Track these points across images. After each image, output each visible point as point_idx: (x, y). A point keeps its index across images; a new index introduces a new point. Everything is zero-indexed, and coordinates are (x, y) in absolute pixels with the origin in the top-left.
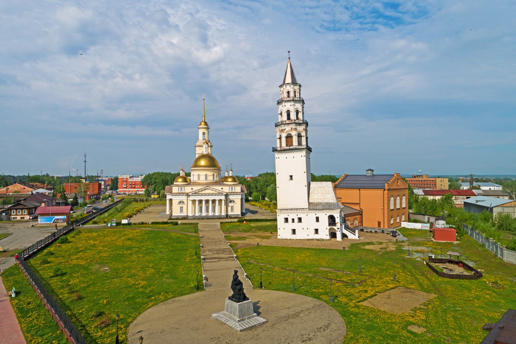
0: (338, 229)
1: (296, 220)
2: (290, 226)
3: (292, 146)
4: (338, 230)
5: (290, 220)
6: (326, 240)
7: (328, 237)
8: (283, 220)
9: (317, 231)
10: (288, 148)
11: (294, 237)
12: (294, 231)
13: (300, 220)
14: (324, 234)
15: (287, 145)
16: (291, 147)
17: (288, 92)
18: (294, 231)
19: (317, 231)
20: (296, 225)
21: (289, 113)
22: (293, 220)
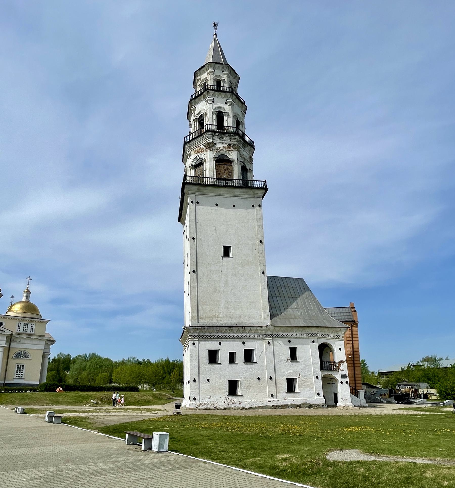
0: (344, 376)
1: (240, 357)
2: (225, 371)
4: (344, 380)
5: (223, 357)
6: (318, 406)
7: (321, 400)
8: (205, 356)
9: (291, 385)
10: (223, 183)
11: (234, 402)
12: (233, 388)
13: (249, 356)
14: (310, 392)
15: (218, 178)
17: (218, 83)
18: (233, 388)
19: (291, 385)
20: (240, 370)
22: (232, 356)
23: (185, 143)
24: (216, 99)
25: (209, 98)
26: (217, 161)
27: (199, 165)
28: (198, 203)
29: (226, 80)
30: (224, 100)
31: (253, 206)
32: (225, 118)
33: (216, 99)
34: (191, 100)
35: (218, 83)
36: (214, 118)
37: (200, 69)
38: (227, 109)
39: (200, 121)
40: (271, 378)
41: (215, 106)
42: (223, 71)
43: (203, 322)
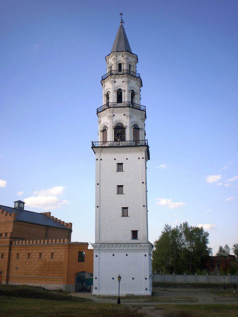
3: (124, 139)
17: (120, 65)
21: (121, 93)
23: (98, 113)
24: (116, 80)
26: (115, 129)
27: (104, 131)
28: (101, 160)
29: (125, 62)
30: (123, 80)
31: (139, 158)
32: (123, 93)
33: (116, 80)
34: (103, 80)
35: (120, 65)
36: (115, 95)
37: (108, 56)
38: (125, 87)
39: (107, 96)
40: (146, 279)
41: (116, 86)
42: (123, 56)
43: (103, 240)
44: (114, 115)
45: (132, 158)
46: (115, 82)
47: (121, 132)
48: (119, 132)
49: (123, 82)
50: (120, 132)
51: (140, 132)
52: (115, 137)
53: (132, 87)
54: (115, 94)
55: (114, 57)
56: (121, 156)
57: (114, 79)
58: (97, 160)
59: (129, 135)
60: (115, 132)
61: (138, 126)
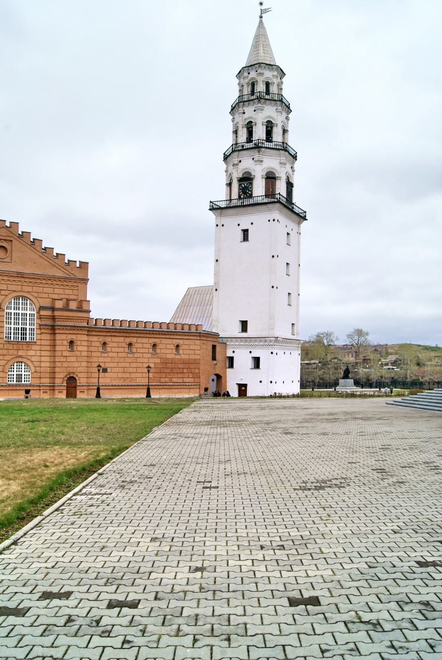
3: (251, 196)
16: (251, 201)
25: (241, 110)
42: (257, 71)
44: (240, 161)
45: (266, 223)
46: (244, 113)
47: (247, 184)
48: (244, 185)
49: (255, 111)
50: (246, 185)
51: (278, 182)
52: (239, 192)
53: (269, 117)
54: (245, 130)
55: (246, 74)
56: (245, 220)
57: (243, 107)
58: (217, 225)
59: (259, 189)
60: (240, 185)
61: (274, 174)
